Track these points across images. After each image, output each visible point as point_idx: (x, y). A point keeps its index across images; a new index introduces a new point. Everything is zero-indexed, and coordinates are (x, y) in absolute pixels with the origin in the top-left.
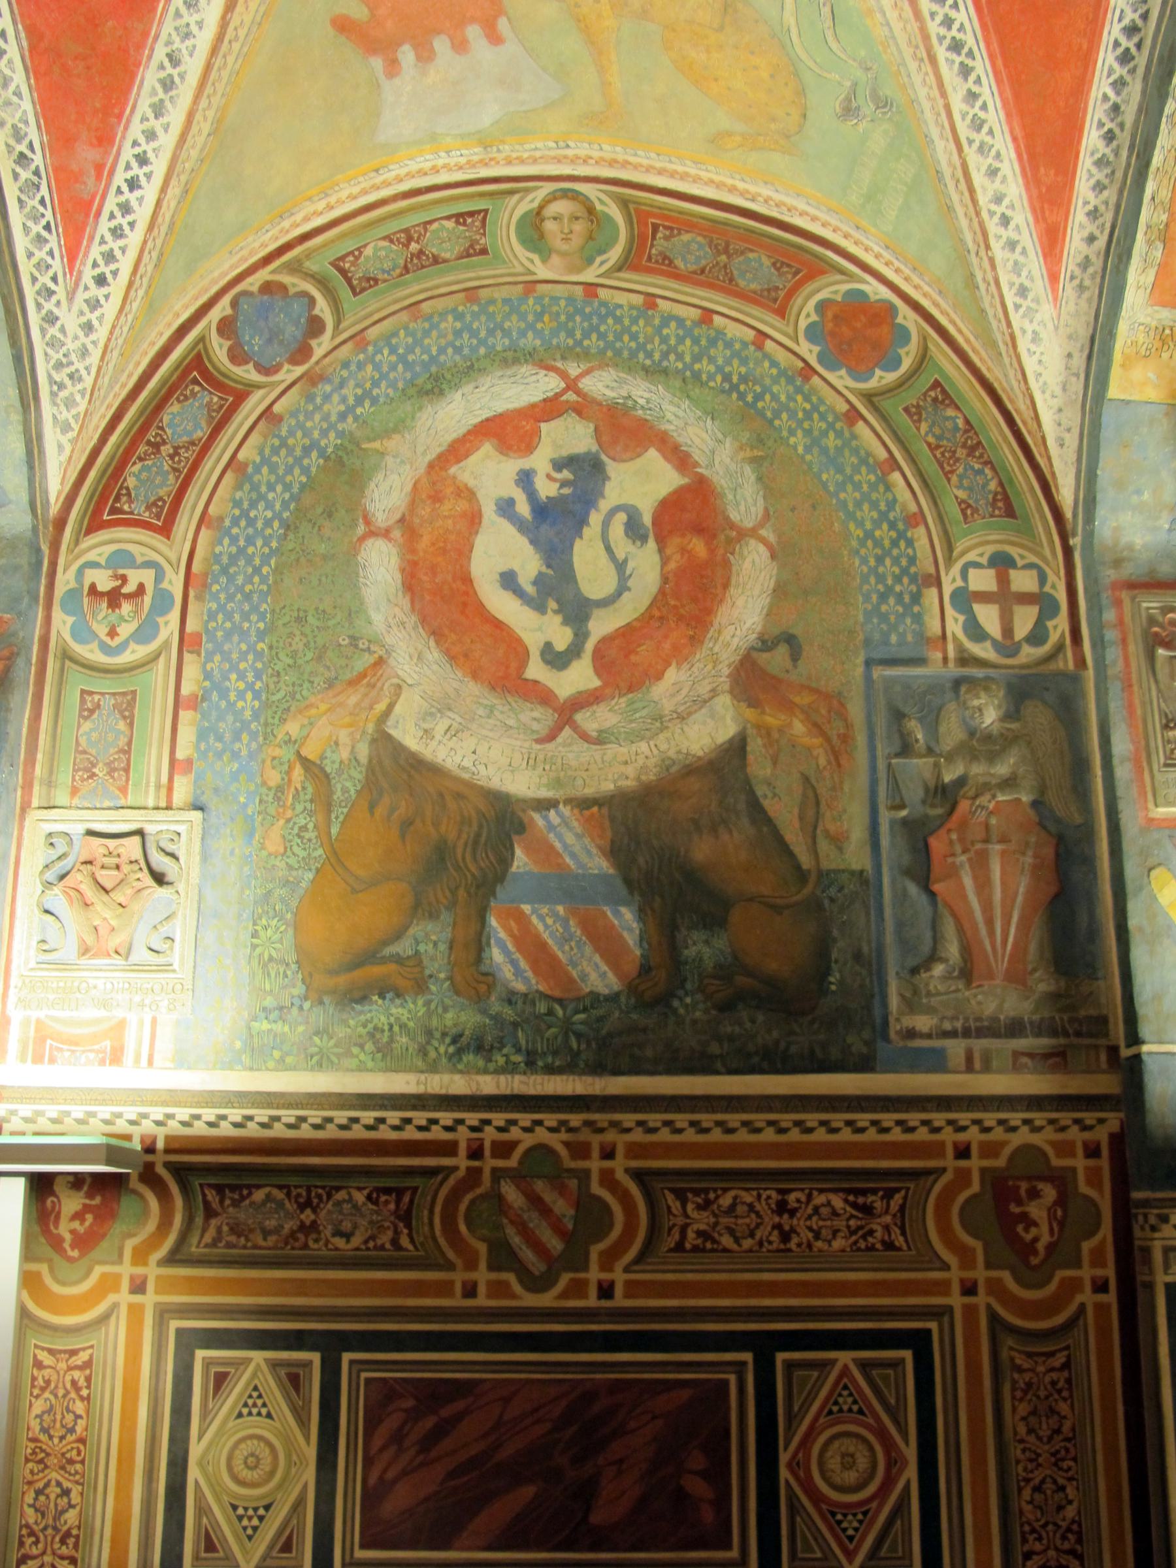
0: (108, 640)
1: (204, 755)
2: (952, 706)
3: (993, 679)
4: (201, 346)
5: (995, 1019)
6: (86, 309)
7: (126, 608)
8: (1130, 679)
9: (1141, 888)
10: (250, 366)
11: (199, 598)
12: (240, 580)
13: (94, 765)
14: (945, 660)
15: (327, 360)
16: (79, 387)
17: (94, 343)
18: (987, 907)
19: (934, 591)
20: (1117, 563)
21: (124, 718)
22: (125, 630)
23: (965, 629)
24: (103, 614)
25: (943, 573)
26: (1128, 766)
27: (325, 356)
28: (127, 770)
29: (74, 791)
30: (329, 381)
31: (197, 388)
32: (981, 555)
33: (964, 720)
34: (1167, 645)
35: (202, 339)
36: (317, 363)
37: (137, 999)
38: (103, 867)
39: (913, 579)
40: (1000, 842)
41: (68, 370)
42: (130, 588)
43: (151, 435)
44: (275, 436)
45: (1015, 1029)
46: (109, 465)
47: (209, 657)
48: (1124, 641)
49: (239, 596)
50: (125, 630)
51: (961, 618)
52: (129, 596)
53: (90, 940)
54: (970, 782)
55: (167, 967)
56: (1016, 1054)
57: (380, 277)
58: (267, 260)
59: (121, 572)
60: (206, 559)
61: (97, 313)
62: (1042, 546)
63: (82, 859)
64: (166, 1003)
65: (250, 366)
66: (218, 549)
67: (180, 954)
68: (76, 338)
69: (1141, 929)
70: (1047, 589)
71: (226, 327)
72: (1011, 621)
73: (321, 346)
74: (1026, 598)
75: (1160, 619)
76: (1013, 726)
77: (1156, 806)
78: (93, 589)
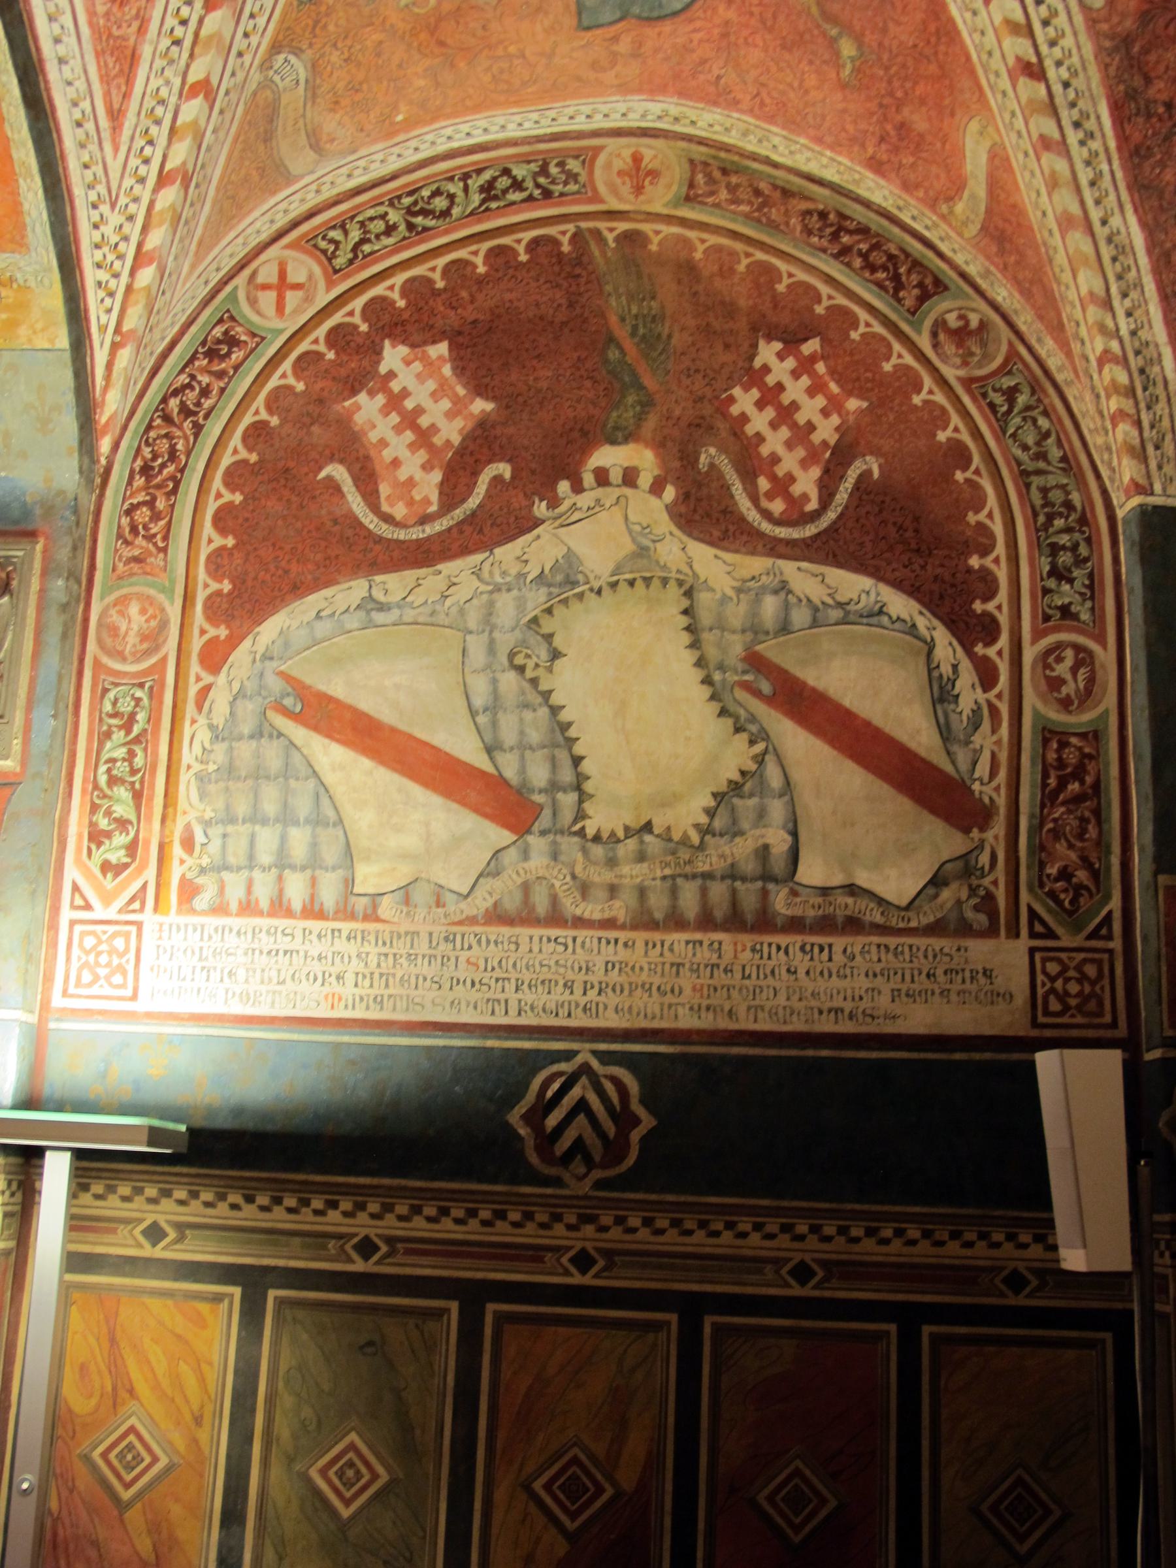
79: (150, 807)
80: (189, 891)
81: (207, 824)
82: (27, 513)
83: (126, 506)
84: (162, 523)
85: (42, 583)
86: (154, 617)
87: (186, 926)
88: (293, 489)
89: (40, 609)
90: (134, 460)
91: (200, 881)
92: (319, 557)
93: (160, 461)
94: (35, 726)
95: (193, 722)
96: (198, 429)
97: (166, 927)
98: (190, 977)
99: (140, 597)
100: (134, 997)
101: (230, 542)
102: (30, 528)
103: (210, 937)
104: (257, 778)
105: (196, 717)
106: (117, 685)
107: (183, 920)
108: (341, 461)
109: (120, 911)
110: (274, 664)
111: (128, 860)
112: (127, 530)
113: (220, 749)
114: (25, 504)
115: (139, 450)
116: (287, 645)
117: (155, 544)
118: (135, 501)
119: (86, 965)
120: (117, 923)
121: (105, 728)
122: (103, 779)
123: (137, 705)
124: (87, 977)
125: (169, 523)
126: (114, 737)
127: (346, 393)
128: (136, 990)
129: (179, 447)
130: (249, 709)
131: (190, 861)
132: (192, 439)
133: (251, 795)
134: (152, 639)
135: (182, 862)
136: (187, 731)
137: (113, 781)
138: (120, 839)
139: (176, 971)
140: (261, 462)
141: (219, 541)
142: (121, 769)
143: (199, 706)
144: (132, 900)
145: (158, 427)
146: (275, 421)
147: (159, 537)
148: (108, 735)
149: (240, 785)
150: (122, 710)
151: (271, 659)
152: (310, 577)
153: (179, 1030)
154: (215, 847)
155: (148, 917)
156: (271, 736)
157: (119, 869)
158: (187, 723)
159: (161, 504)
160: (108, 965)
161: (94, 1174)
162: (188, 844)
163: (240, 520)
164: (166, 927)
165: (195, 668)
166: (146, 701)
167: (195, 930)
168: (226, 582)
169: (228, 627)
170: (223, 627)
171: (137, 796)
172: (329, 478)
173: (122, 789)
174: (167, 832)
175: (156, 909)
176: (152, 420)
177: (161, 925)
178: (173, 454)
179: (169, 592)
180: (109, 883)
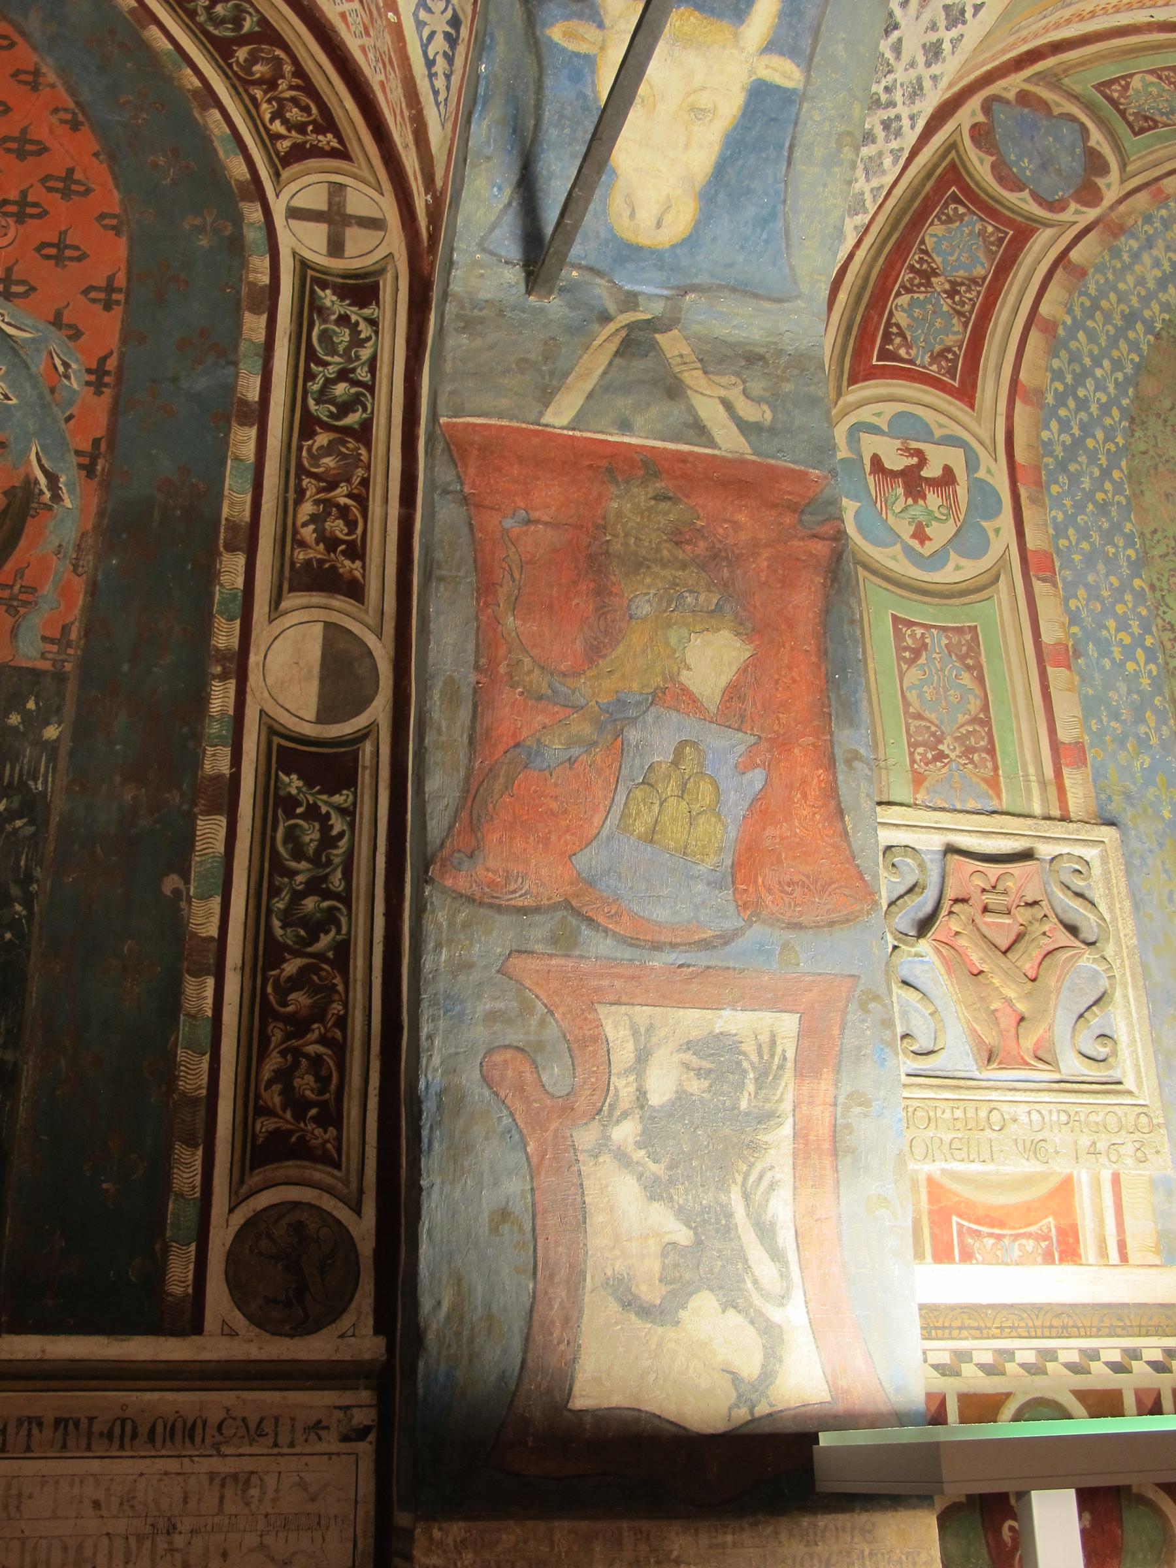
0: (915, 543)
1: (1099, 736)
4: (953, 154)
6: (942, 22)
7: (933, 499)
10: (1026, 194)
11: (1036, 501)
12: (1086, 483)
13: (940, 741)
15: (1122, 208)
16: (894, 145)
17: (934, 78)
21: (968, 668)
22: (940, 533)
24: (898, 507)
27: (1120, 201)
28: (991, 751)
29: (918, 780)
30: (1134, 236)
31: (961, 210)
35: (952, 146)
36: (1112, 208)
37: (1085, 1140)
38: (986, 910)
41: (884, 114)
42: (932, 471)
43: (914, 258)
44: (1081, 294)
46: (863, 288)
47: (1070, 595)
49: (1090, 506)
50: (940, 533)
52: (934, 483)
53: (990, 1038)
55: (1113, 1085)
57: (1158, 118)
58: (1020, 63)
59: (914, 445)
60: (1030, 446)
61: (954, 33)
63: (950, 894)
64: (1129, 1149)
65: (1026, 194)
66: (1045, 435)
67: (1133, 1062)
68: (913, 64)
71: (982, 135)
73: (1111, 187)
78: (876, 461)
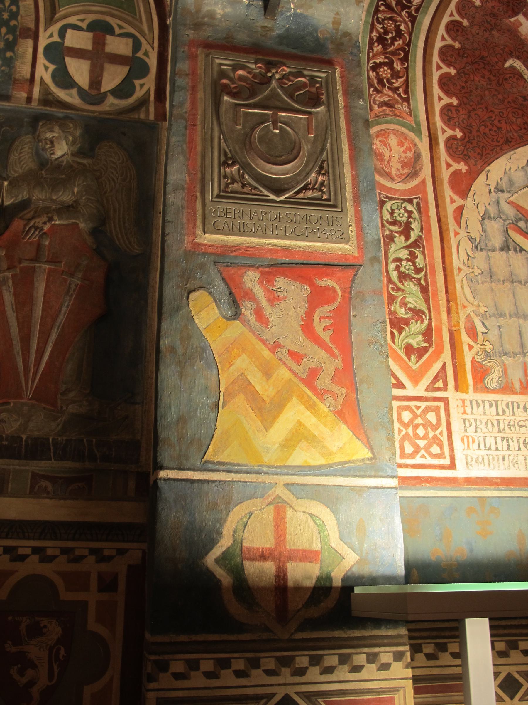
2: (27, 138)
3: (72, 119)
5: (15, 439)
8: (195, 120)
9: (178, 310)
14: (29, 100)
18: (25, 325)
19: (30, 43)
20: (198, 26)
23: (54, 77)
25: (41, 29)
26: (181, 194)
32: (82, 20)
33: (37, 153)
34: (233, 95)
39: (12, 30)
40: (48, 262)
45: (37, 449)
48: (194, 88)
51: (52, 67)
54: (33, 206)
56: (35, 477)
62: (141, 22)
69: (173, 350)
70: (140, 54)
72: (101, 75)
74: (117, 59)
75: (232, 75)
76: (85, 161)
77: (205, 233)
79: (437, 301)
80: (480, 374)
81: (483, 316)
82: (320, 45)
83: (371, 64)
84: (401, 80)
85: (345, 101)
86: (410, 150)
87: (483, 401)
88: (490, 71)
89: (349, 122)
90: (371, 32)
91: (487, 364)
92: (519, 121)
93: (390, 35)
94: (365, 218)
95: (456, 234)
96: (413, 19)
97: (467, 403)
98: (493, 447)
99: (395, 132)
100: (452, 466)
101: (455, 101)
102: (326, 57)
103: (504, 412)
104: (512, 282)
105: (458, 230)
106: (391, 199)
107: (480, 397)
108: (518, 59)
109: (427, 389)
110: (506, 195)
111: (427, 345)
112: (375, 81)
113: (481, 256)
114: (317, 39)
115: (373, 25)
116: (511, 182)
117: (399, 95)
118: (378, 61)
119: (406, 437)
120: (427, 399)
121: (387, 233)
122: (394, 275)
123: (409, 217)
124: (409, 449)
125: (407, 80)
126: (396, 240)
127: (510, 13)
128: (453, 458)
129: (402, 28)
130: (495, 228)
131: (476, 347)
132: (410, 24)
133: (511, 295)
134: (412, 167)
135: (470, 347)
136: (453, 241)
137: (403, 277)
138: (417, 327)
139: (481, 439)
140: (463, 48)
141: (446, 100)
142: (407, 267)
143: (459, 224)
144: (436, 379)
145: (383, 11)
146: (465, 23)
147: (401, 90)
148: (391, 239)
149: (501, 286)
150: (399, 219)
151: (502, 191)
152: (515, 134)
153: (496, 494)
154: (493, 334)
155: (450, 393)
156: (515, 250)
157: (421, 352)
158: (452, 235)
159: (397, 66)
160: (425, 437)
161: (448, 633)
162: (472, 333)
163: (459, 87)
164: (467, 403)
165: (448, 192)
166: (416, 215)
167: (491, 406)
168: (457, 130)
169: (466, 164)
170: (462, 163)
171: (424, 290)
172: (512, 67)
173: (411, 284)
174: (454, 322)
175: (457, 388)
176: (378, 6)
177: (463, 401)
178: (399, 34)
179: (417, 131)
180: (414, 364)
